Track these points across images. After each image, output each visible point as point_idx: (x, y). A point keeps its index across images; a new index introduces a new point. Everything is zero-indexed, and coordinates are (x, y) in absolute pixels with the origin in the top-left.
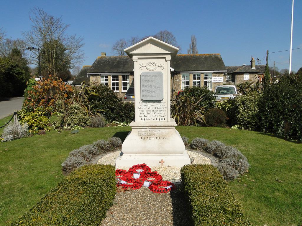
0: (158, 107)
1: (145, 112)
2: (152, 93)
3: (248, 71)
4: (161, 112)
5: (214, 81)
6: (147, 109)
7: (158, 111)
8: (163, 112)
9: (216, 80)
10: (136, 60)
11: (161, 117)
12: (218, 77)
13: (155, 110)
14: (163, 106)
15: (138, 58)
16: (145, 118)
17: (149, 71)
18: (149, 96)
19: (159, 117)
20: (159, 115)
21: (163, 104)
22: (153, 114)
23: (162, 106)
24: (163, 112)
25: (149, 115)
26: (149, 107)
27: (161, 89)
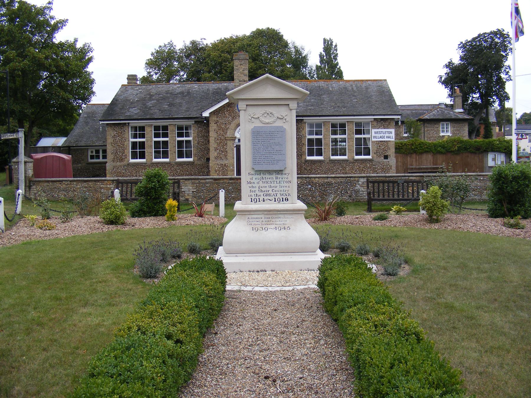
0: (278, 180)
1: (257, 189)
2: (268, 159)
3: (448, 117)
4: (282, 189)
5: (375, 137)
6: (261, 184)
7: (278, 187)
8: (285, 189)
9: (379, 135)
10: (243, 109)
11: (282, 197)
12: (384, 130)
13: (272, 185)
14: (286, 180)
15: (247, 105)
16: (257, 198)
17: (264, 125)
18: (264, 164)
19: (279, 196)
20: (280, 192)
21: (286, 176)
22: (270, 192)
23: (284, 180)
24: (285, 189)
25: (264, 193)
26: (263, 180)
27: (282, 152)
